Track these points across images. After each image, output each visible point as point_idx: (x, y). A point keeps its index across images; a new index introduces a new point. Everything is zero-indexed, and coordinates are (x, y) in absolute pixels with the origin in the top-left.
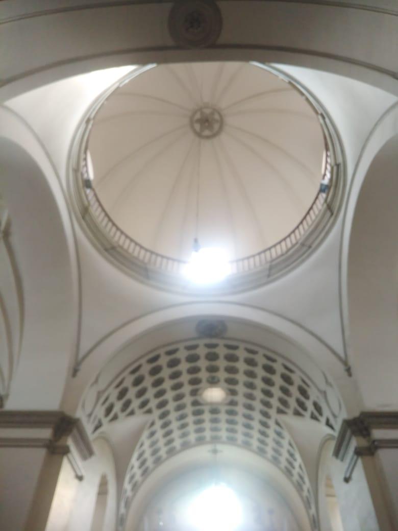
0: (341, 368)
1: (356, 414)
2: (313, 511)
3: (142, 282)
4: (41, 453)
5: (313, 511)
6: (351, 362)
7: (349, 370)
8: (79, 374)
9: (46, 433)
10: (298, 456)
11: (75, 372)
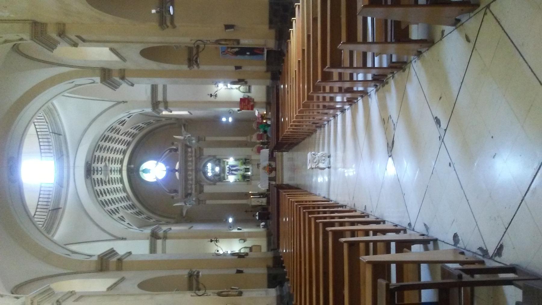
0: (122, 105)
1: (150, 106)
2: (164, 119)
3: (63, 211)
4: (168, 241)
5: (164, 119)
6: (121, 100)
7: (124, 102)
8: (124, 237)
9: (159, 242)
10: (138, 125)
11: (123, 239)
